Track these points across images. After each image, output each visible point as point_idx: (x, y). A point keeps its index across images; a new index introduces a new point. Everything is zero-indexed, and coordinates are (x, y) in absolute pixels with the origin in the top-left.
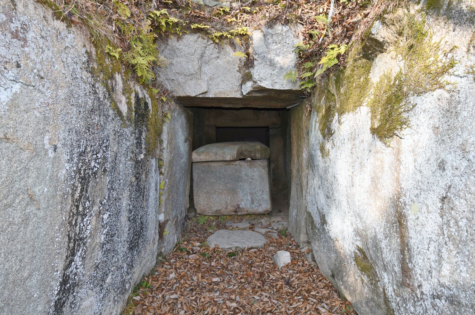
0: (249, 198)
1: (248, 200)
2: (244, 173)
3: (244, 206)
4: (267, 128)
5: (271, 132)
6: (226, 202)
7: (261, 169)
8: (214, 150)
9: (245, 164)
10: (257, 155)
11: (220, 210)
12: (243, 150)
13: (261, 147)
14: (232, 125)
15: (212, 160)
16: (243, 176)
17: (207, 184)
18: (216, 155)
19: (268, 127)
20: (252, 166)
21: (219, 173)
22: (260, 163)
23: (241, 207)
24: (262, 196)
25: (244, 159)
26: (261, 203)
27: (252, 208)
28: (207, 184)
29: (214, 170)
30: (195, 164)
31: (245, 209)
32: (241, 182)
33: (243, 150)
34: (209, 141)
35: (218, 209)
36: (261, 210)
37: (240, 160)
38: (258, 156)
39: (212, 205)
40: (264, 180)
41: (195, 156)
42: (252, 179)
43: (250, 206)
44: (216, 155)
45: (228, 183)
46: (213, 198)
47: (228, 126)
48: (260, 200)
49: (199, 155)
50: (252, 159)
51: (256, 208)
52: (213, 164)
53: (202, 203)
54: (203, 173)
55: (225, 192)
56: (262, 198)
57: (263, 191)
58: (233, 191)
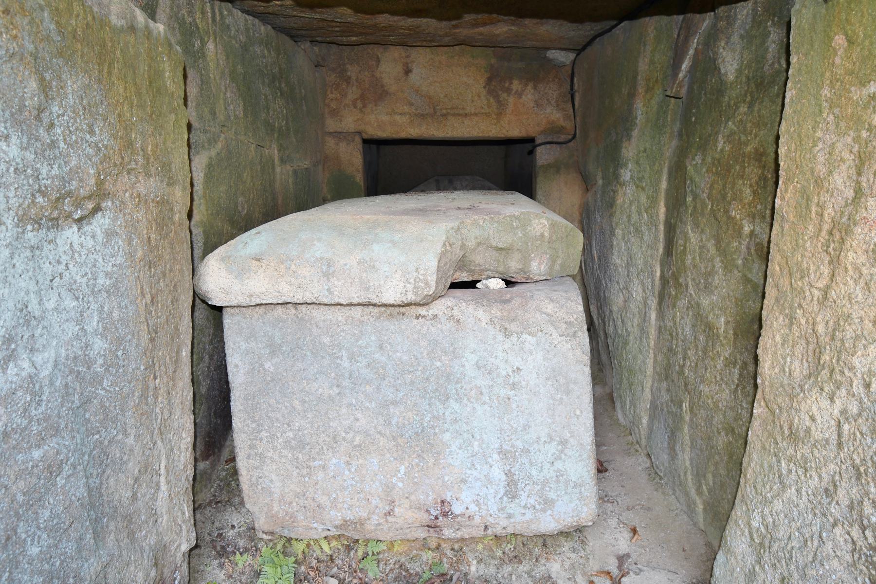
0: (498, 473)
1: (489, 481)
2: (470, 359)
3: (473, 508)
4: (528, 143)
5: (543, 156)
6: (389, 489)
7: (556, 338)
8: (319, 250)
9: (480, 313)
11: (361, 523)
12: (471, 244)
13: (553, 225)
14: (414, 132)
15: (309, 298)
16: (470, 370)
17: (297, 404)
18: (327, 275)
19: (530, 140)
20: (513, 327)
21: (352, 357)
22: (549, 308)
23: (457, 509)
24: (559, 465)
25: (471, 285)
26: (552, 495)
27: (510, 516)
28: (297, 404)
29: (326, 340)
30: (229, 310)
31: (477, 520)
32: (459, 400)
33: (471, 244)
34: (342, 191)
35: (349, 516)
37: (455, 286)
38: (538, 267)
39: (323, 500)
40: (568, 392)
41: (219, 278)
42: (514, 386)
43: (502, 509)
44: (327, 275)
45: (395, 403)
46: (324, 468)
47: (403, 135)
48: (545, 483)
49: (241, 273)
50: (509, 283)
51: (529, 516)
52: (318, 314)
53: (276, 487)
54: (273, 353)
55: (382, 441)
56: (560, 474)
57: (563, 443)
58: (421, 443)
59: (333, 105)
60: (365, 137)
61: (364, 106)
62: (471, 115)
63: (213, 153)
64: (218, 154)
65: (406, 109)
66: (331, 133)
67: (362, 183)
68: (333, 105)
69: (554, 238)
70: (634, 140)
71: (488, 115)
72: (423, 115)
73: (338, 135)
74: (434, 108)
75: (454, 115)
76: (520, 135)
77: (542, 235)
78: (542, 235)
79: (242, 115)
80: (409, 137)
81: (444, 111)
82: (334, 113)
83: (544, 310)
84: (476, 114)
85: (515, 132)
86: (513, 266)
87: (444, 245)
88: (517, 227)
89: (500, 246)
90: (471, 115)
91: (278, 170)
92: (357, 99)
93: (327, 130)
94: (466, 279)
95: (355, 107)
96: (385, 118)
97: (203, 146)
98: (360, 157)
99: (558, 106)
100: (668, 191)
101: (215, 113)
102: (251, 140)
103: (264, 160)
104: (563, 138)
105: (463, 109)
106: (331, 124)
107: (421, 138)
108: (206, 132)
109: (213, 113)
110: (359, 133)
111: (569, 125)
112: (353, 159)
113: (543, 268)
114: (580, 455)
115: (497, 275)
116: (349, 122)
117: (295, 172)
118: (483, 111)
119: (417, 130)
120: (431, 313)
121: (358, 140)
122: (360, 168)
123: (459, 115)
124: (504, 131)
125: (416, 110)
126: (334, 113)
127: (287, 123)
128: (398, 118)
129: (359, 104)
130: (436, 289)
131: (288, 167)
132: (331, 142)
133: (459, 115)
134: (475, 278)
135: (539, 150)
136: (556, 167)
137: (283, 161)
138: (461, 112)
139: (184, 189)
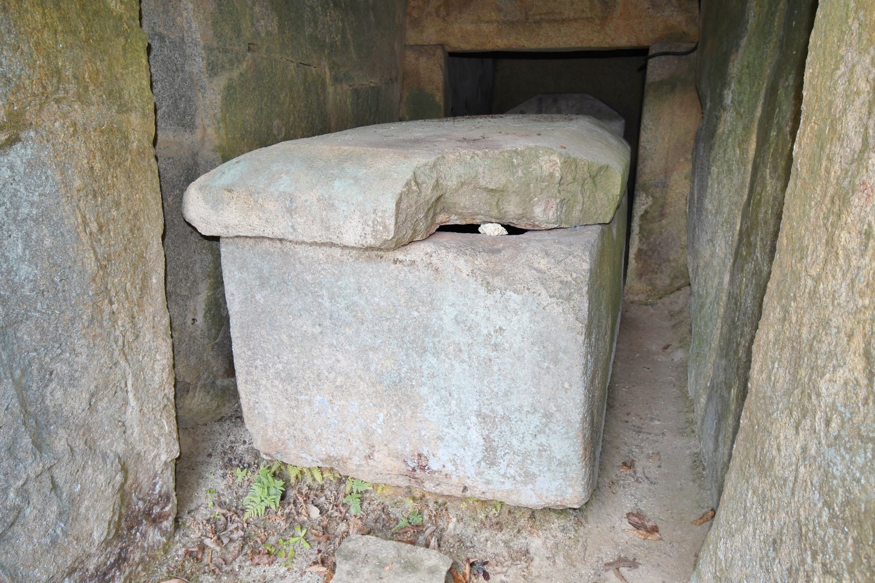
0: (475, 436)
1: (466, 443)
2: (448, 313)
3: (450, 467)
6: (369, 433)
7: (545, 299)
8: (284, 184)
9: (461, 263)
10: (538, 211)
11: (343, 461)
13: (569, 163)
14: (501, 43)
16: (448, 324)
17: (284, 337)
18: (290, 211)
20: (497, 282)
21: (332, 298)
22: (543, 263)
23: (434, 465)
24: (542, 439)
26: (533, 469)
27: (488, 482)
28: (284, 337)
29: (309, 277)
31: (454, 480)
32: (436, 354)
33: (451, 183)
34: (420, 110)
35: (333, 453)
36: (529, 497)
39: (310, 433)
40: (556, 362)
42: (496, 347)
43: (480, 474)
44: (290, 211)
45: (374, 349)
46: (310, 402)
47: (489, 47)
48: (526, 455)
49: (216, 204)
50: (512, 230)
51: (508, 485)
52: (298, 248)
53: (270, 413)
54: (262, 285)
55: (362, 386)
56: (542, 449)
57: (548, 416)
58: (399, 392)
59: (415, 14)
60: (449, 50)
61: (448, 14)
62: (570, 20)
63: (235, 74)
64: (241, 74)
65: (494, 15)
66: (412, 46)
67: (442, 104)
68: (415, 14)
69: (570, 178)
70: (741, 51)
71: (589, 20)
72: (512, 23)
73: (421, 49)
74: (526, 14)
75: (549, 21)
76: (629, 44)
77: (551, 175)
78: (551, 175)
79: (276, 31)
80: (496, 49)
81: (538, 17)
82: (416, 23)
83: (536, 265)
84: (575, 20)
85: (623, 41)
86: (513, 211)
87: (408, 184)
88: (518, 165)
89: (491, 187)
90: (570, 20)
91: (330, 90)
92: (439, 7)
93: (407, 43)
94: (458, 223)
95: (438, 16)
96: (470, 27)
97: (223, 67)
98: (440, 73)
99: (680, 6)
100: (761, 119)
101: (240, 31)
102: (290, 58)
103: (309, 79)
104: (684, 47)
105: (561, 13)
106: (412, 37)
107: (509, 50)
108: (226, 51)
109: (237, 30)
110: (442, 45)
111: (693, 31)
112: (433, 74)
113: (551, 214)
114: (567, 433)
115: (493, 220)
116: (430, 34)
117: (356, 92)
118: (584, 15)
119: (505, 42)
120: (408, 258)
121: (439, 52)
122: (441, 86)
123: (555, 21)
124: (609, 40)
125: (505, 16)
126: (416, 23)
127: (344, 37)
128: (484, 27)
129: (443, 12)
130: (396, 233)
131: (346, 87)
132: (411, 56)
133: (555, 21)
134: (469, 221)
135: (651, 63)
136: (670, 85)
137: (336, 80)
138: (558, 17)
139: (144, 116)
